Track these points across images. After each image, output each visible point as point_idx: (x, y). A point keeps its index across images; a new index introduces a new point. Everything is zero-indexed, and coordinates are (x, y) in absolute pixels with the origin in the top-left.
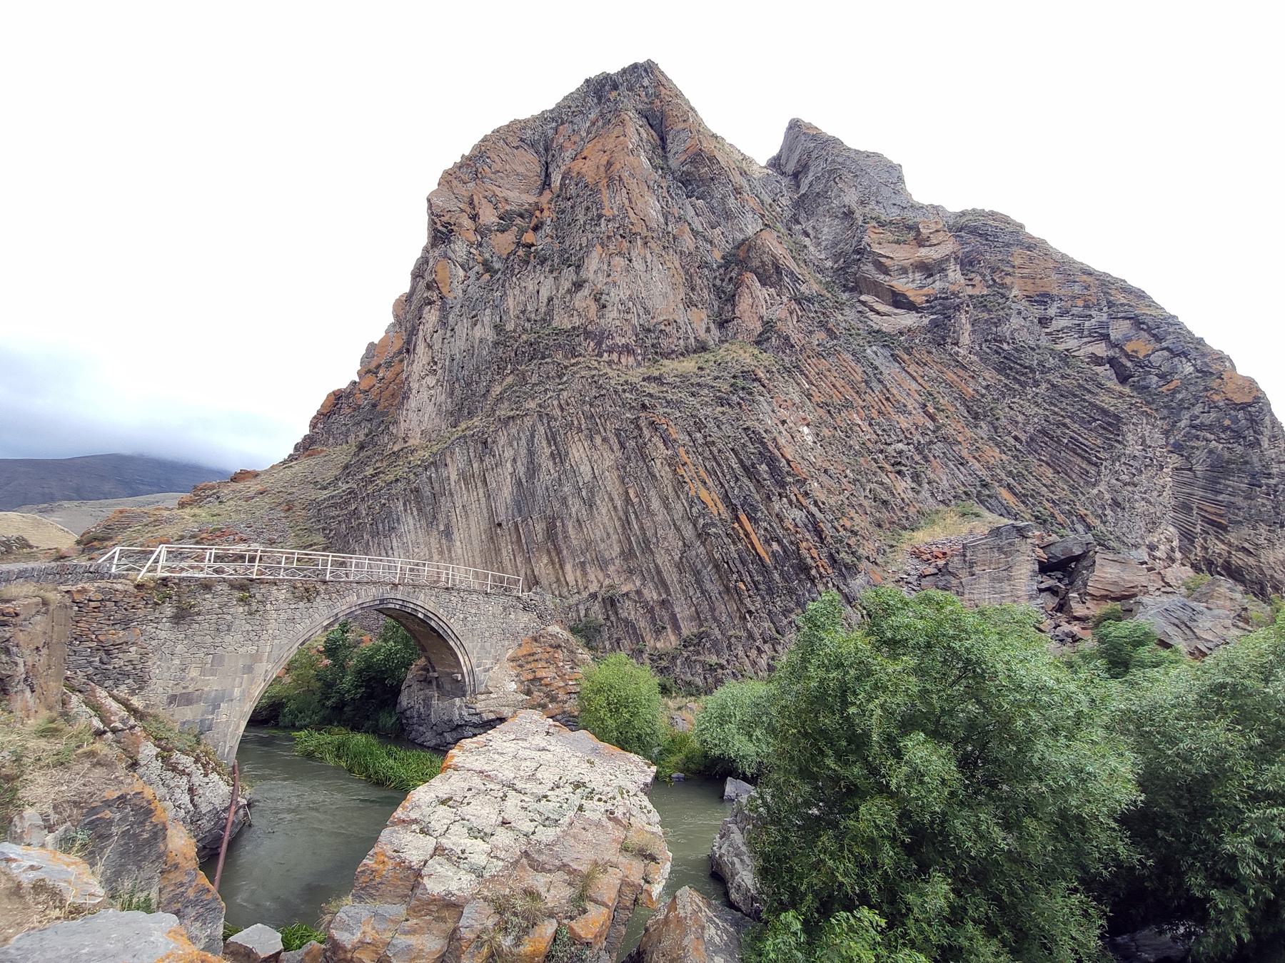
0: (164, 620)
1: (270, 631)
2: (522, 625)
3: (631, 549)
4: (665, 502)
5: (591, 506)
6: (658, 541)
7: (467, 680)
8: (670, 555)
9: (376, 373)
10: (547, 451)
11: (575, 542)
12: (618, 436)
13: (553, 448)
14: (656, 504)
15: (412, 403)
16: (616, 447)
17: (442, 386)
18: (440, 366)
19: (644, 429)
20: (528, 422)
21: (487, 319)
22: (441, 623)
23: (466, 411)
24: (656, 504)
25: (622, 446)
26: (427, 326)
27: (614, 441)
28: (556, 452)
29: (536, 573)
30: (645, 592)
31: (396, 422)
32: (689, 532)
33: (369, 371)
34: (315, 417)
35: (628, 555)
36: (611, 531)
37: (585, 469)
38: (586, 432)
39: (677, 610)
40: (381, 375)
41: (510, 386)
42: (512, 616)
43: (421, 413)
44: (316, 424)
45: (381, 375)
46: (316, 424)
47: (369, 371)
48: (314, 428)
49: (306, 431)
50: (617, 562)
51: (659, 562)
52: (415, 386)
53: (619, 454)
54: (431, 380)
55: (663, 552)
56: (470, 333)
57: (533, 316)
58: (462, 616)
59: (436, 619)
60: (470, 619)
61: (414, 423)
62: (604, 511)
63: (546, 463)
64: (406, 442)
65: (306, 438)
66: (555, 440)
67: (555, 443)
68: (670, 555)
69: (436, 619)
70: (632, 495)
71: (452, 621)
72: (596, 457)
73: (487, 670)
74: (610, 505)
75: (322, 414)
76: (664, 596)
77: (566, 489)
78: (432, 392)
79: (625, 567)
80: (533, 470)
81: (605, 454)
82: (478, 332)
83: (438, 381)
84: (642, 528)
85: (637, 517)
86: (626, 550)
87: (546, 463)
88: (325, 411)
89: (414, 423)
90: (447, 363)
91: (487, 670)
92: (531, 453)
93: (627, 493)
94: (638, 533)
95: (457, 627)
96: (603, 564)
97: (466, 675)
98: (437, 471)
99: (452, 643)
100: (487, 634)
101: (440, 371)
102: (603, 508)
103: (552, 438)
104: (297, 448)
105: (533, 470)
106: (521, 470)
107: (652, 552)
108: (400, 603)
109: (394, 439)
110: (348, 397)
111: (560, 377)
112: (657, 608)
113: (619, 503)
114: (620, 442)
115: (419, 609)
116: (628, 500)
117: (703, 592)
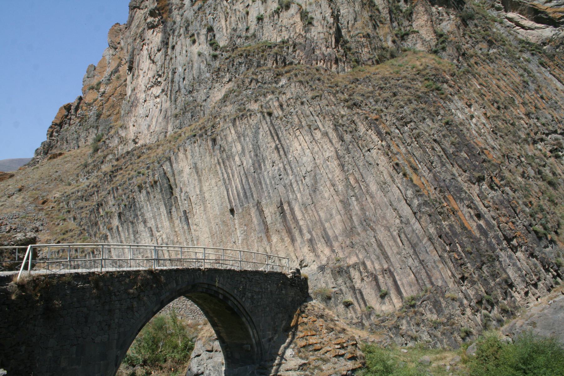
0: (39, 317)
1: (116, 320)
2: (290, 299)
3: (353, 228)
4: (383, 186)
5: (315, 191)
6: (378, 220)
7: (256, 350)
8: (389, 231)
9: (98, 89)
10: (274, 145)
11: (301, 223)
12: (336, 130)
13: (277, 142)
14: (373, 188)
15: (141, 110)
16: (335, 140)
17: (166, 95)
18: (164, 78)
19: (359, 124)
20: (254, 121)
21: (202, 38)
22: (236, 302)
23: (190, 114)
24: (373, 188)
25: (342, 139)
26: (151, 46)
27: (333, 135)
28: (279, 146)
29: (268, 249)
30: (368, 264)
31: (123, 127)
32: (406, 211)
33: (92, 88)
34: (51, 127)
35: (350, 231)
36: (334, 212)
37: (307, 159)
38: (307, 128)
39: (397, 278)
40: (102, 90)
41: (231, 91)
42: (283, 292)
43: (148, 119)
44: (52, 132)
45: (102, 90)
46: (52, 132)
47: (92, 88)
48: (51, 135)
49: (44, 138)
50: (340, 239)
51: (380, 237)
52: (142, 96)
53: (338, 146)
54: (157, 91)
55: (382, 229)
56: (189, 50)
57: (244, 34)
58: (250, 295)
59: (232, 299)
60: (255, 297)
61: (144, 128)
62: (326, 195)
63: (270, 154)
64: (136, 143)
65: (43, 144)
66: (277, 135)
67: (278, 138)
68: (389, 231)
69: (232, 299)
70: (352, 181)
71: (244, 299)
72: (316, 149)
73: (270, 340)
74: (332, 189)
75: (56, 124)
76: (386, 266)
77: (291, 177)
78: (158, 100)
79: (348, 242)
80: (258, 162)
81: (325, 147)
82: (195, 49)
83: (163, 91)
84: (362, 209)
85: (357, 200)
86: (348, 228)
87: (270, 154)
88: (58, 122)
89: (144, 128)
90: (170, 76)
91: (270, 340)
92: (257, 147)
93: (347, 179)
94: (359, 213)
95: (248, 305)
96: (328, 241)
97: (255, 346)
98: (171, 165)
99: (244, 319)
100: (268, 309)
101: (164, 83)
102: (326, 192)
103: (275, 134)
104: (37, 152)
105: (258, 162)
106: (248, 162)
107: (373, 230)
108: (206, 286)
109: (122, 141)
110: (77, 109)
111: (276, 83)
112: (380, 277)
113: (340, 187)
114: (338, 135)
115: (221, 292)
116: (348, 185)
117: (421, 262)
